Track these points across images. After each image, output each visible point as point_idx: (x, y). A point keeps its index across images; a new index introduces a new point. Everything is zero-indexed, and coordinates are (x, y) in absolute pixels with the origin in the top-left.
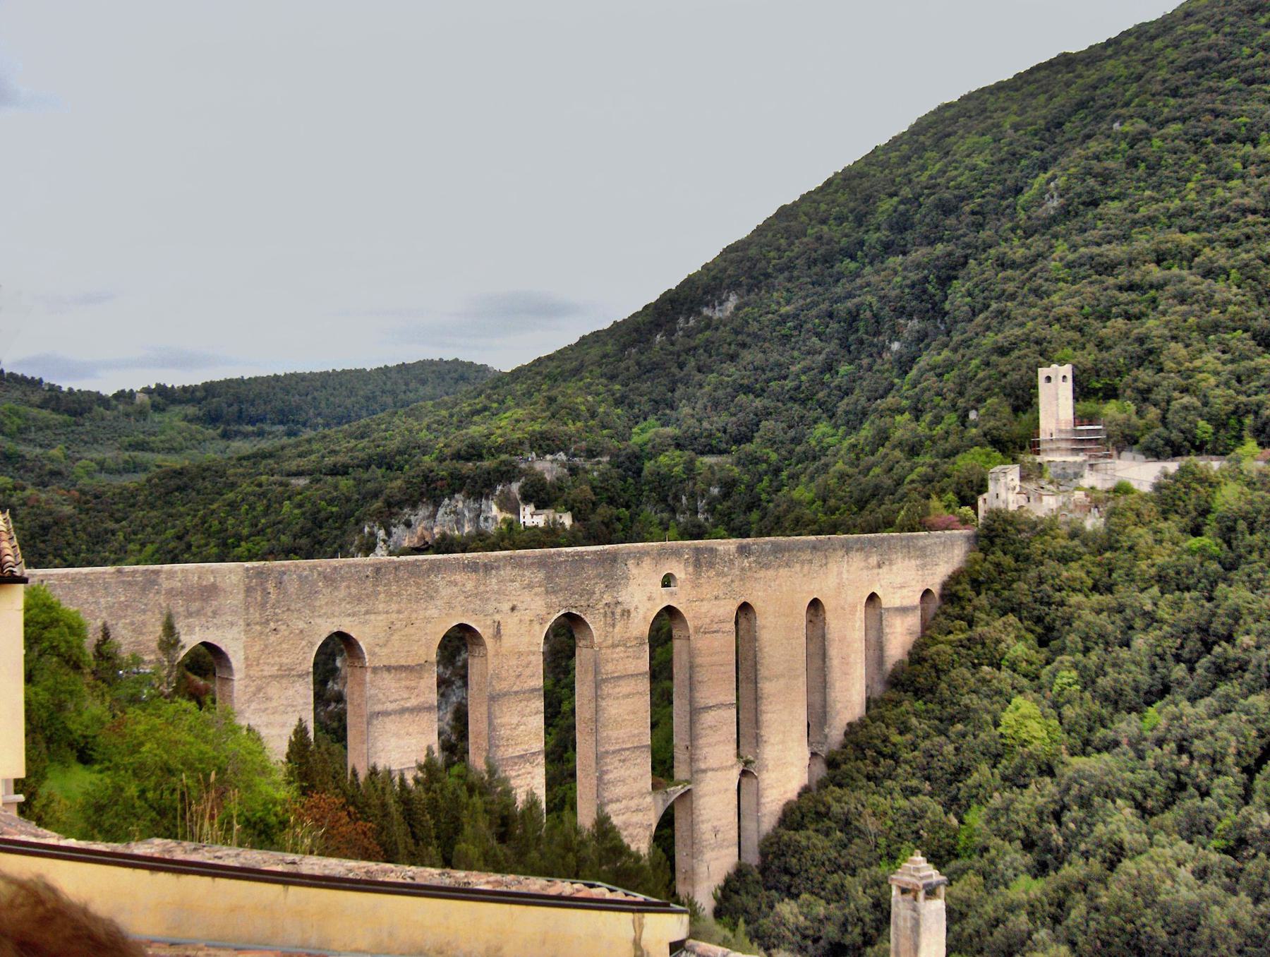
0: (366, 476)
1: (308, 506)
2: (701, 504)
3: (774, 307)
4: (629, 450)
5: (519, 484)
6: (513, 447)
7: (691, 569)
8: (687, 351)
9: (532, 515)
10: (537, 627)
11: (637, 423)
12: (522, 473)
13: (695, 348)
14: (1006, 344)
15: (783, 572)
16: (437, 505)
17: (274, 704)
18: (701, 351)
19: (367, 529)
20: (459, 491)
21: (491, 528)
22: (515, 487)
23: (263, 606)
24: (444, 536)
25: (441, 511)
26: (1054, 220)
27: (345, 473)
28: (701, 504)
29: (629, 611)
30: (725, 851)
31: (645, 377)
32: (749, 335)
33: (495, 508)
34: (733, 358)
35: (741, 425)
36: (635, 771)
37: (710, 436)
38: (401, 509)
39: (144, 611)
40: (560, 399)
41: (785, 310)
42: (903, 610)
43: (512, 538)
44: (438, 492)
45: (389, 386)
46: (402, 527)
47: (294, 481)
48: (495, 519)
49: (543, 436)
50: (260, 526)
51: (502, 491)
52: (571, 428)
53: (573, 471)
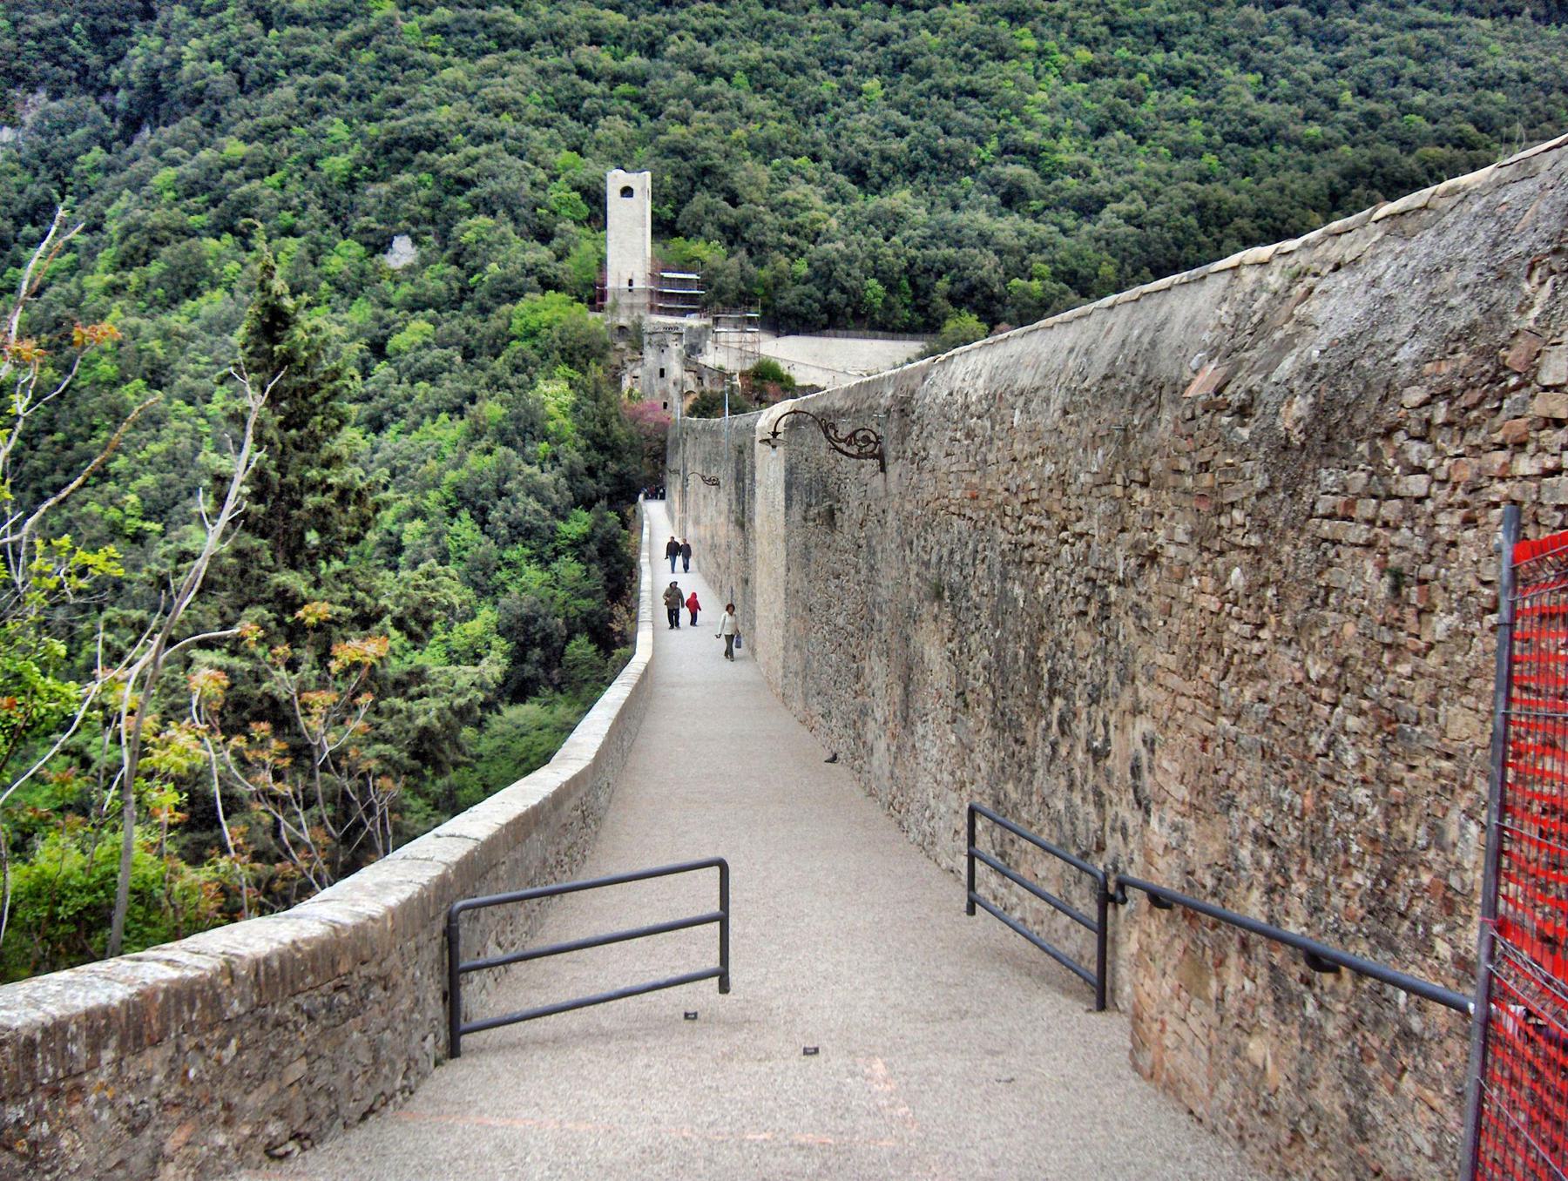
14: (428, 134)
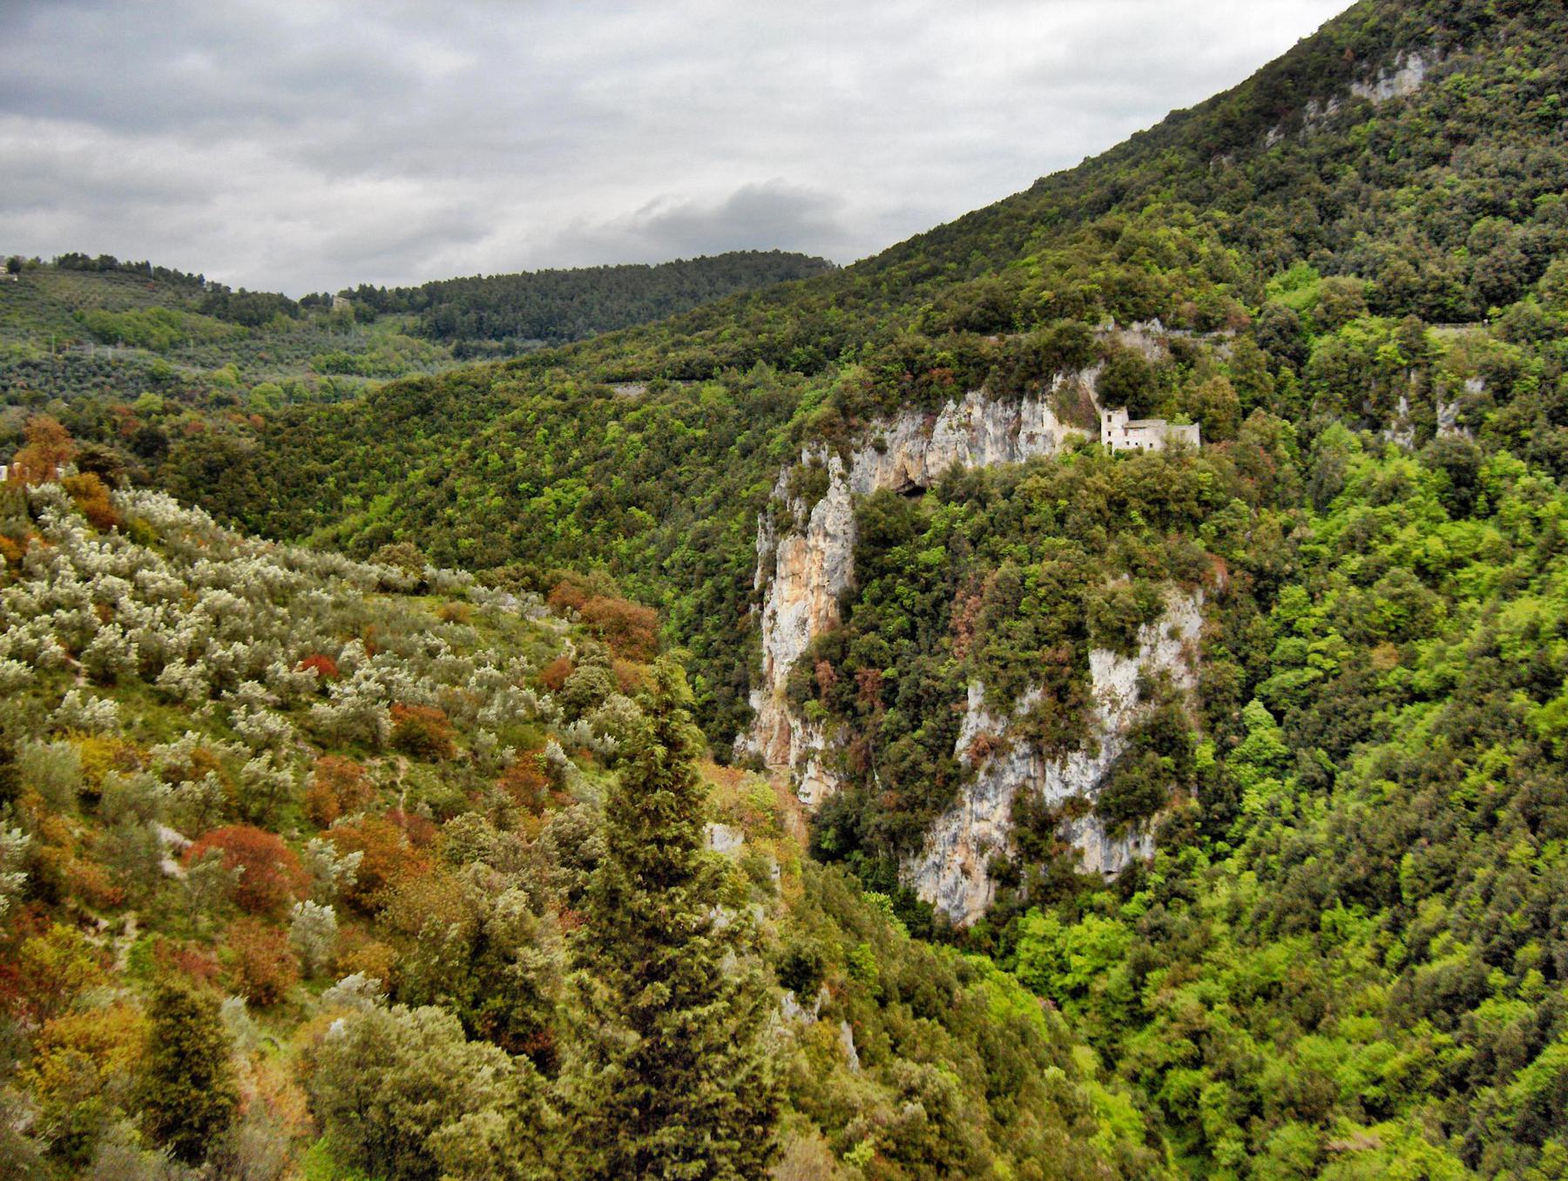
0: (743, 381)
1: (652, 428)
2: (1446, 413)
3: (1511, 71)
4: (1278, 317)
5: (1096, 372)
6: (1079, 305)
8: (1337, 155)
9: (1126, 430)
11: (1271, 274)
12: (1098, 350)
13: (1352, 149)
16: (932, 413)
18: (1367, 152)
19: (806, 457)
20: (975, 387)
22: (1088, 379)
24: (956, 472)
25: (942, 423)
27: (707, 376)
31: (1266, 197)
32: (1467, 120)
33: (1049, 418)
34: (1441, 159)
35: (1501, 269)
37: (1442, 289)
38: (867, 419)
40: (1128, 230)
41: (1537, 74)
44: (935, 389)
45: (687, 286)
46: (871, 452)
47: (619, 390)
48: (1049, 438)
49: (1126, 288)
50: (571, 461)
51: (1063, 386)
52: (1166, 278)
53: (1177, 351)
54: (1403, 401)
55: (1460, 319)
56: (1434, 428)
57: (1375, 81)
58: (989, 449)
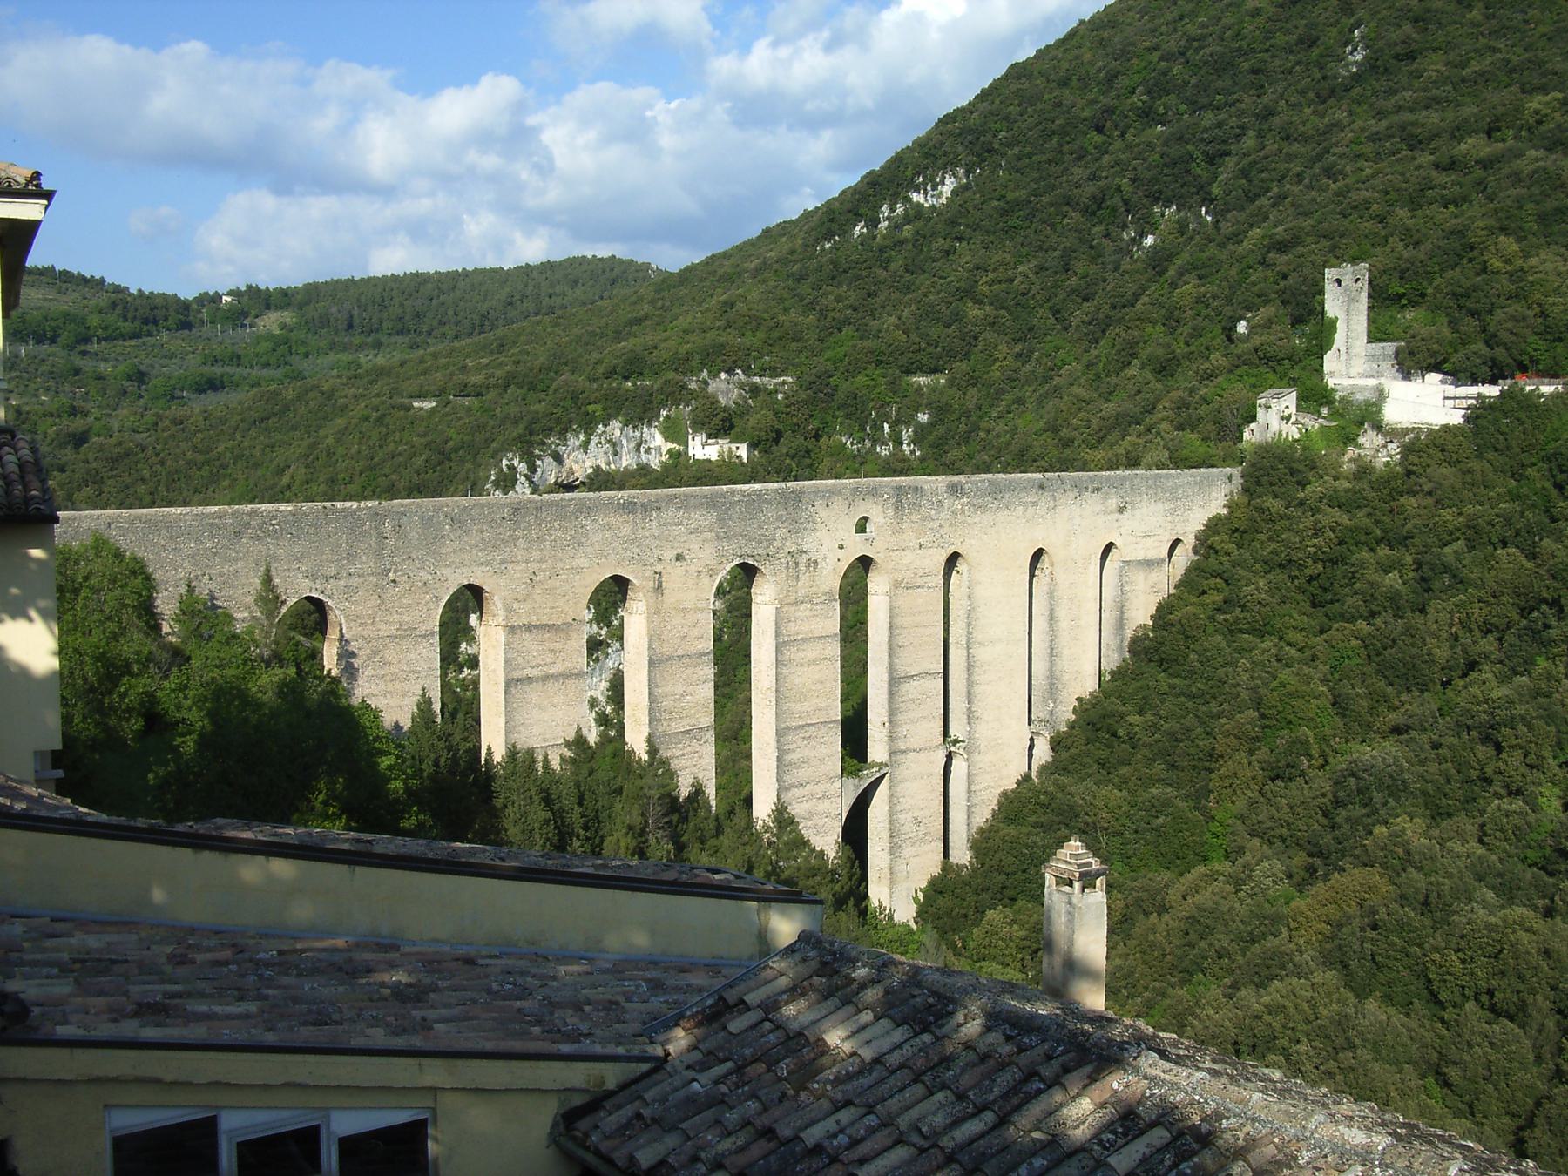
7: (891, 512)
9: (704, 445)
10: (706, 580)
15: (1002, 516)
16: (589, 432)
17: (393, 669)
18: (910, 247)
19: (505, 462)
20: (616, 417)
21: (654, 462)
23: (379, 554)
24: (597, 469)
25: (594, 440)
26: (1357, 78)
28: (908, 432)
29: (816, 562)
30: (928, 847)
36: (824, 751)
39: (236, 560)
41: (1010, 196)
42: (1148, 564)
43: (680, 472)
46: (548, 460)
48: (658, 450)
49: (719, 349)
51: (668, 417)
53: (755, 390)
54: (886, 426)
55: (934, 371)
56: (901, 443)
57: (926, 193)
58: (624, 458)
